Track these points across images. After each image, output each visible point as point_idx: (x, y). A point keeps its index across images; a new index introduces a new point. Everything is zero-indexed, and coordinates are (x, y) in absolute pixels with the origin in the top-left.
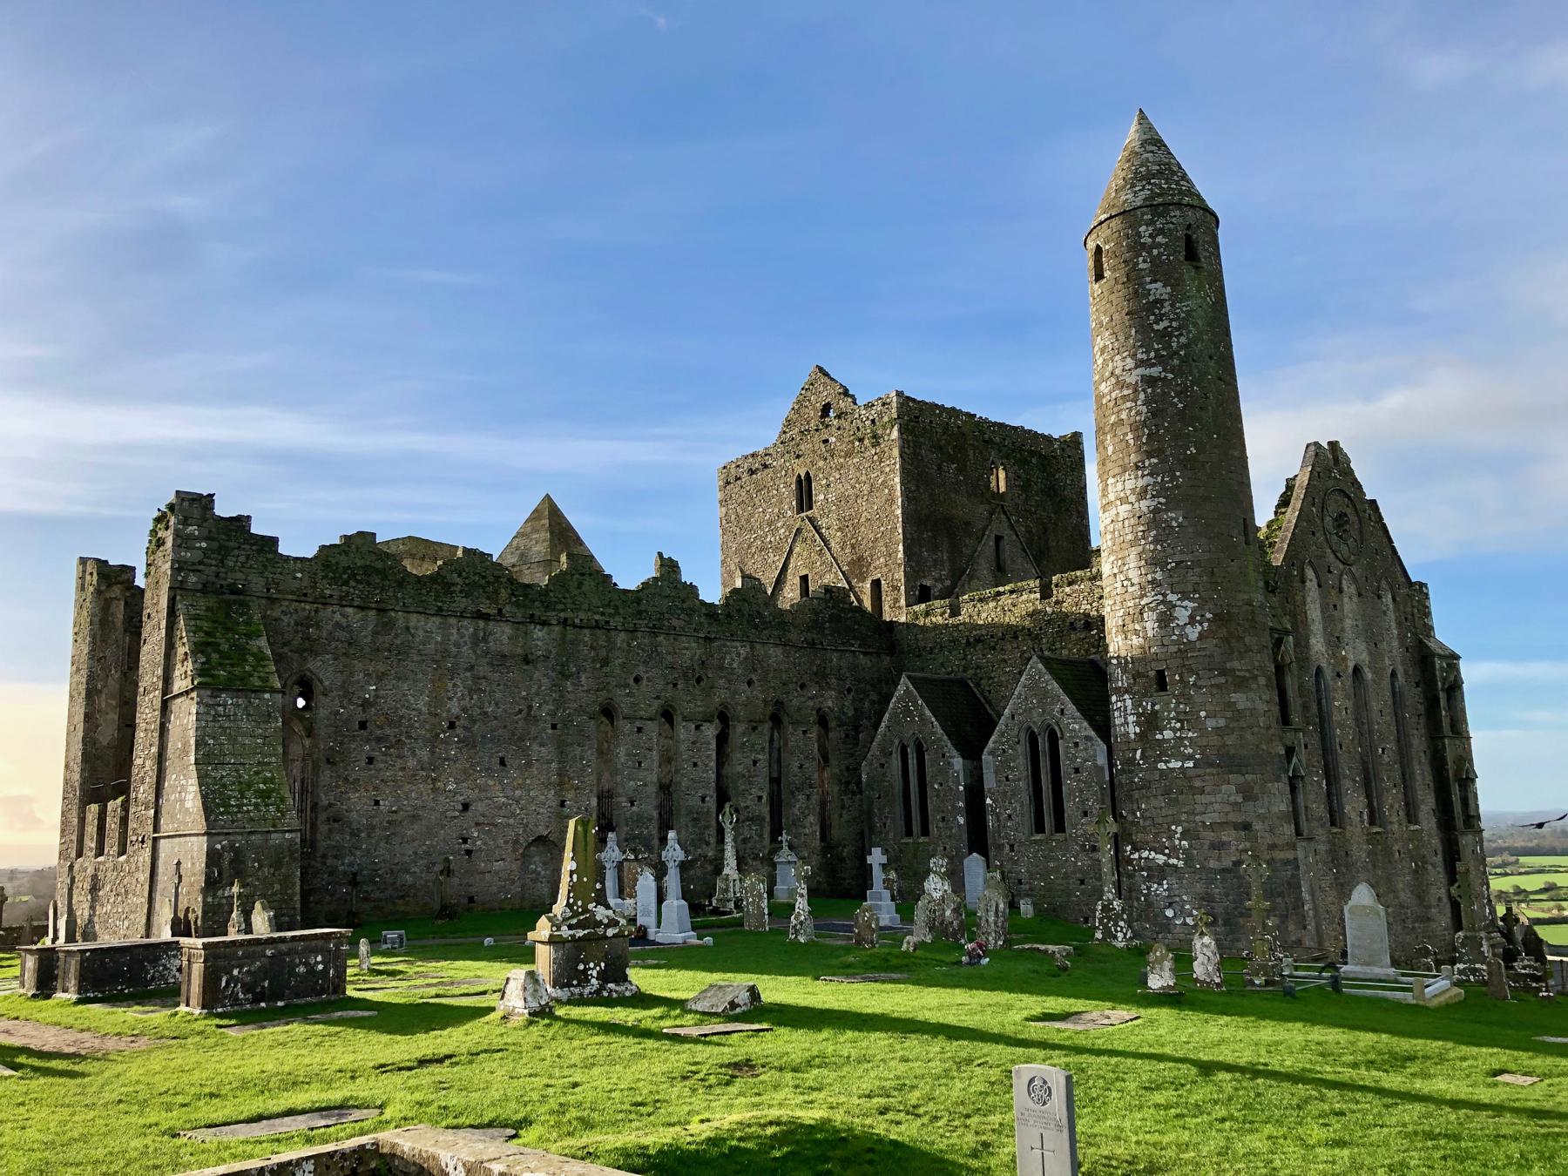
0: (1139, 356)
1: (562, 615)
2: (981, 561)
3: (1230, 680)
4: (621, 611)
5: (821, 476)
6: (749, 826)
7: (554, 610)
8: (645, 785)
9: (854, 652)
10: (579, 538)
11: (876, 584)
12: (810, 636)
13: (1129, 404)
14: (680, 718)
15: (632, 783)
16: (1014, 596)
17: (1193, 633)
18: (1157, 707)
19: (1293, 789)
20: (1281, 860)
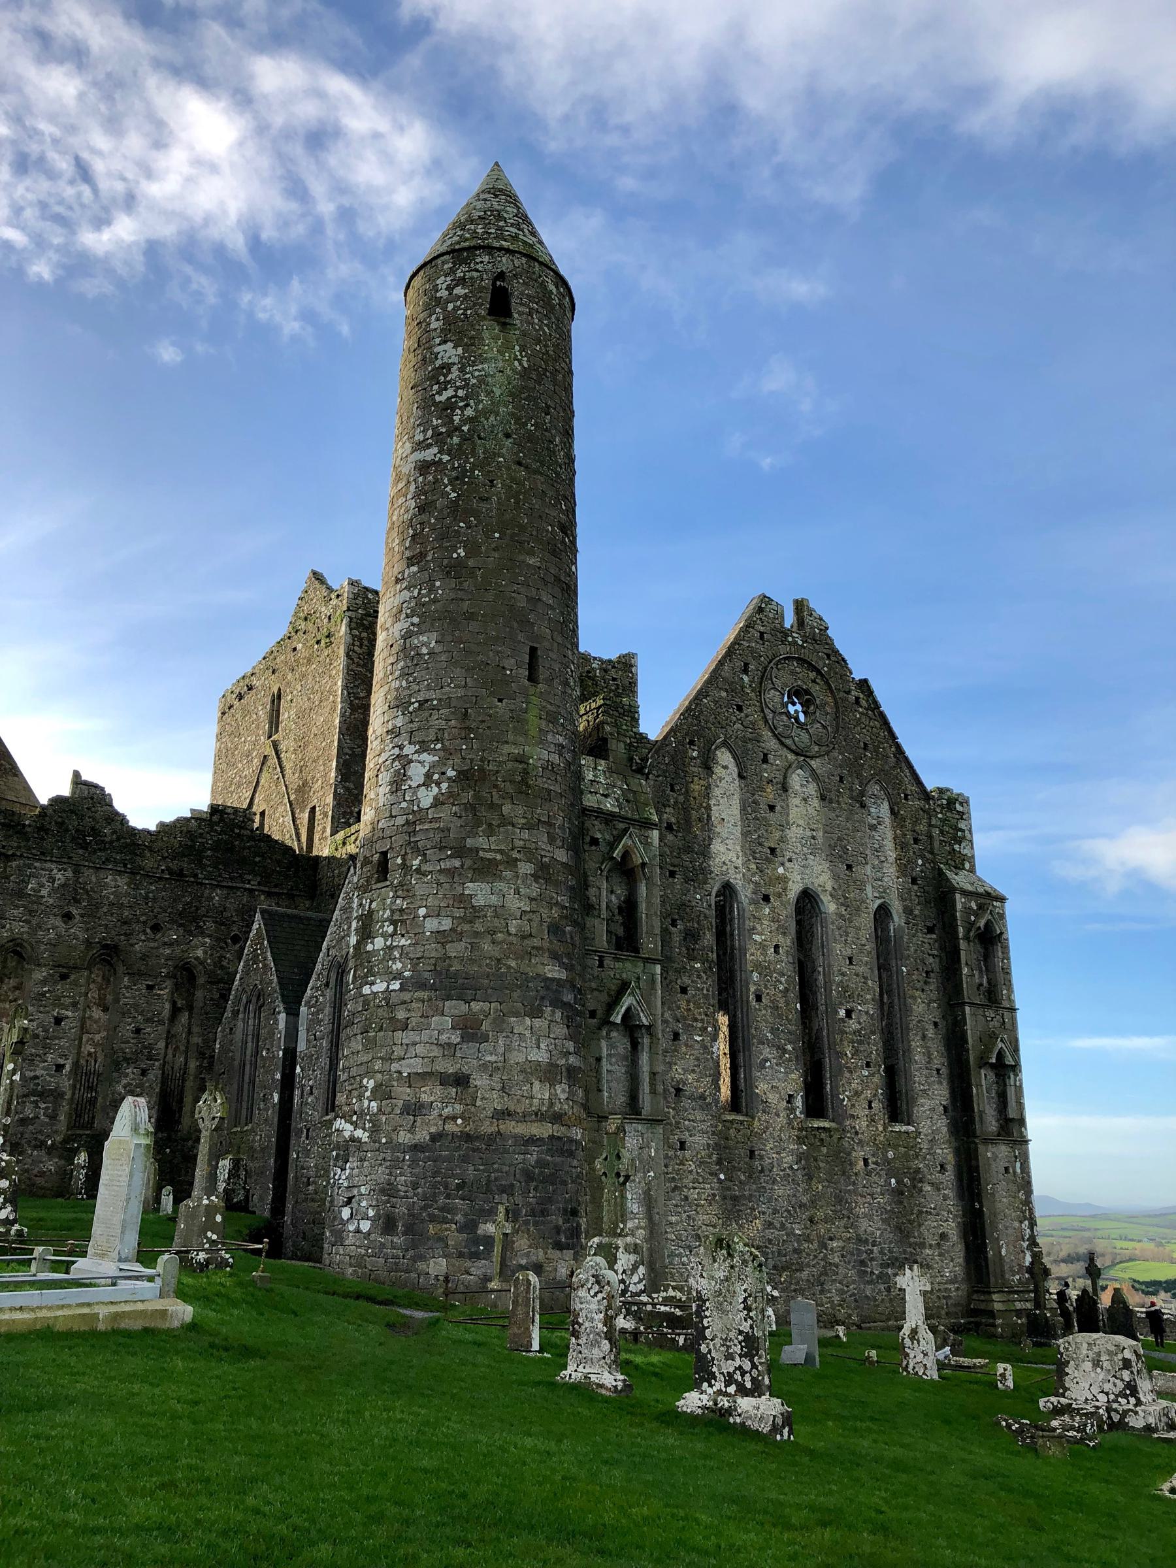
0: (417, 438)
3: (468, 862)
6: (36, 1102)
9: (251, 891)
12: (174, 866)
17: (426, 798)
20: (516, 1137)
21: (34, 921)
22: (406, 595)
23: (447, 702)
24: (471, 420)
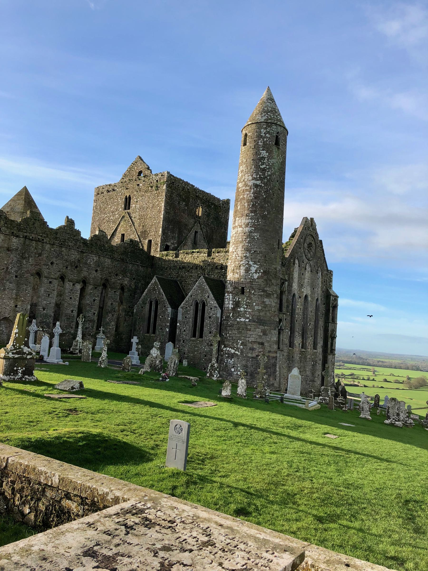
0: (254, 176)
1: (25, 234)
2: (189, 239)
4: (49, 236)
5: (135, 197)
7: (22, 232)
8: (50, 303)
10: (36, 205)
11: (150, 241)
13: (248, 193)
14: (67, 280)
15: (45, 302)
16: (198, 254)
17: (256, 276)
18: (240, 300)
19: (279, 333)
20: (272, 357)
21: (89, 272)
22: (250, 221)
23: (261, 252)
24: (270, 176)
